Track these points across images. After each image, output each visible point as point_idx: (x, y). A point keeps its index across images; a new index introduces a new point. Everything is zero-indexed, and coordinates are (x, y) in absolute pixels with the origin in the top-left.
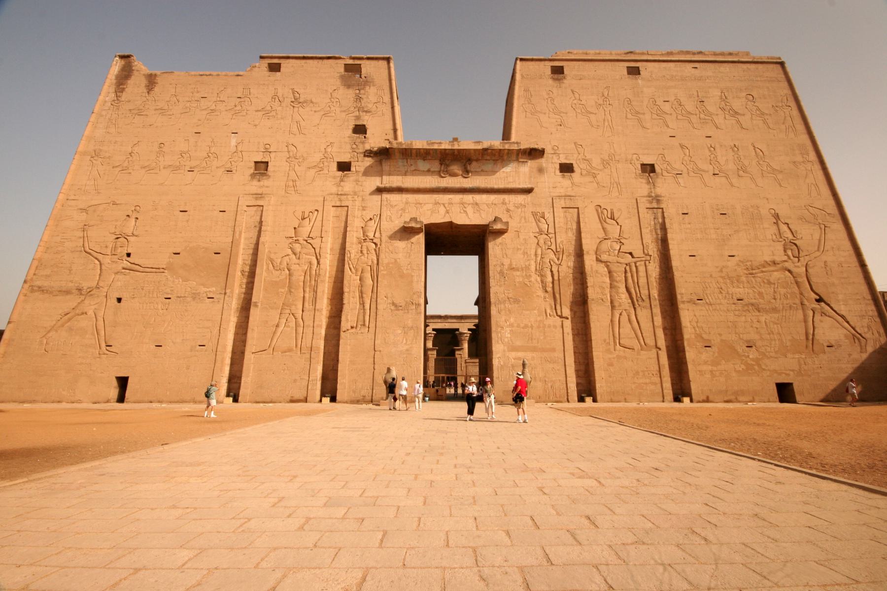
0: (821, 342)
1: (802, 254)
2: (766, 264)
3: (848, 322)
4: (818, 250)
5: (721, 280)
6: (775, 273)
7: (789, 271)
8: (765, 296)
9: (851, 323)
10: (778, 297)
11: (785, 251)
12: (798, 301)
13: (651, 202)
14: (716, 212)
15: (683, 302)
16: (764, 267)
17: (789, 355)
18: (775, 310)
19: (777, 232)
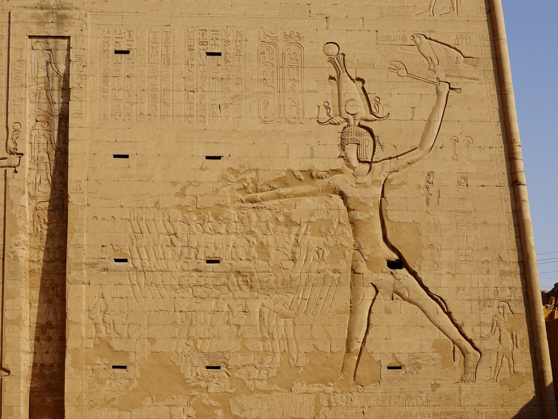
0: (377, 358)
1: (380, 154)
2: (292, 177)
3: (449, 314)
4: (421, 146)
5: (179, 215)
6: (308, 200)
7: (342, 195)
8: (272, 251)
9: (455, 316)
10: (301, 254)
11: (342, 146)
12: (345, 266)
13: (41, 23)
14: (197, 47)
15: (78, 266)
16: (286, 185)
17: (299, 387)
18: (288, 285)
19: (333, 102)
